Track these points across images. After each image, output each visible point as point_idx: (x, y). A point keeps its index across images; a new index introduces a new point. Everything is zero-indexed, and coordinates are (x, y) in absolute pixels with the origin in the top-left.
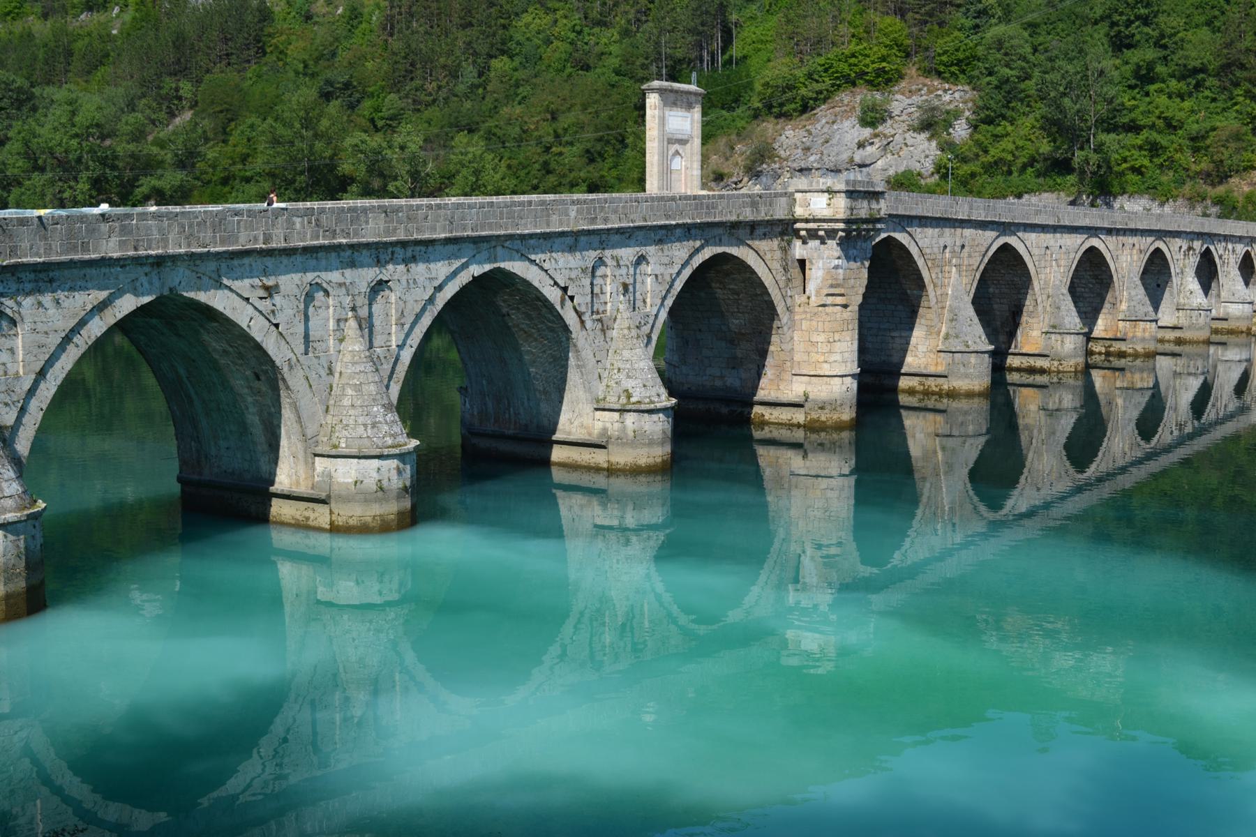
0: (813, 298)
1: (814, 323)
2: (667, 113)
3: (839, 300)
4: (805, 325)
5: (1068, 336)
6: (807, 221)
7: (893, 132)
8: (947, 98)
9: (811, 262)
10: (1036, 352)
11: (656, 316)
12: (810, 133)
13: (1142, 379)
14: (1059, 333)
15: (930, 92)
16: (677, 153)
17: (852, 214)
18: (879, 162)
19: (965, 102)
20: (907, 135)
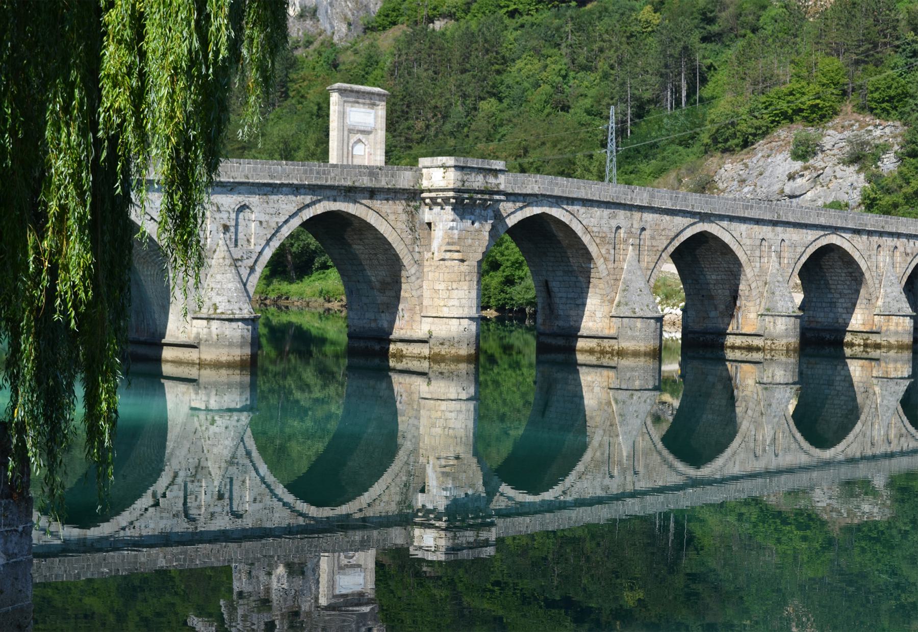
0: (436, 254)
1: (437, 274)
2: (348, 108)
3: (456, 255)
4: (431, 275)
5: (780, 318)
6: (430, 191)
7: (823, 165)
8: (878, 133)
9: (435, 224)
10: (753, 332)
11: (260, 253)
12: (746, 166)
13: (896, 369)
14: (772, 315)
15: (861, 127)
16: (359, 141)
17: (463, 185)
18: (809, 194)
19: (895, 137)
20: (837, 168)
